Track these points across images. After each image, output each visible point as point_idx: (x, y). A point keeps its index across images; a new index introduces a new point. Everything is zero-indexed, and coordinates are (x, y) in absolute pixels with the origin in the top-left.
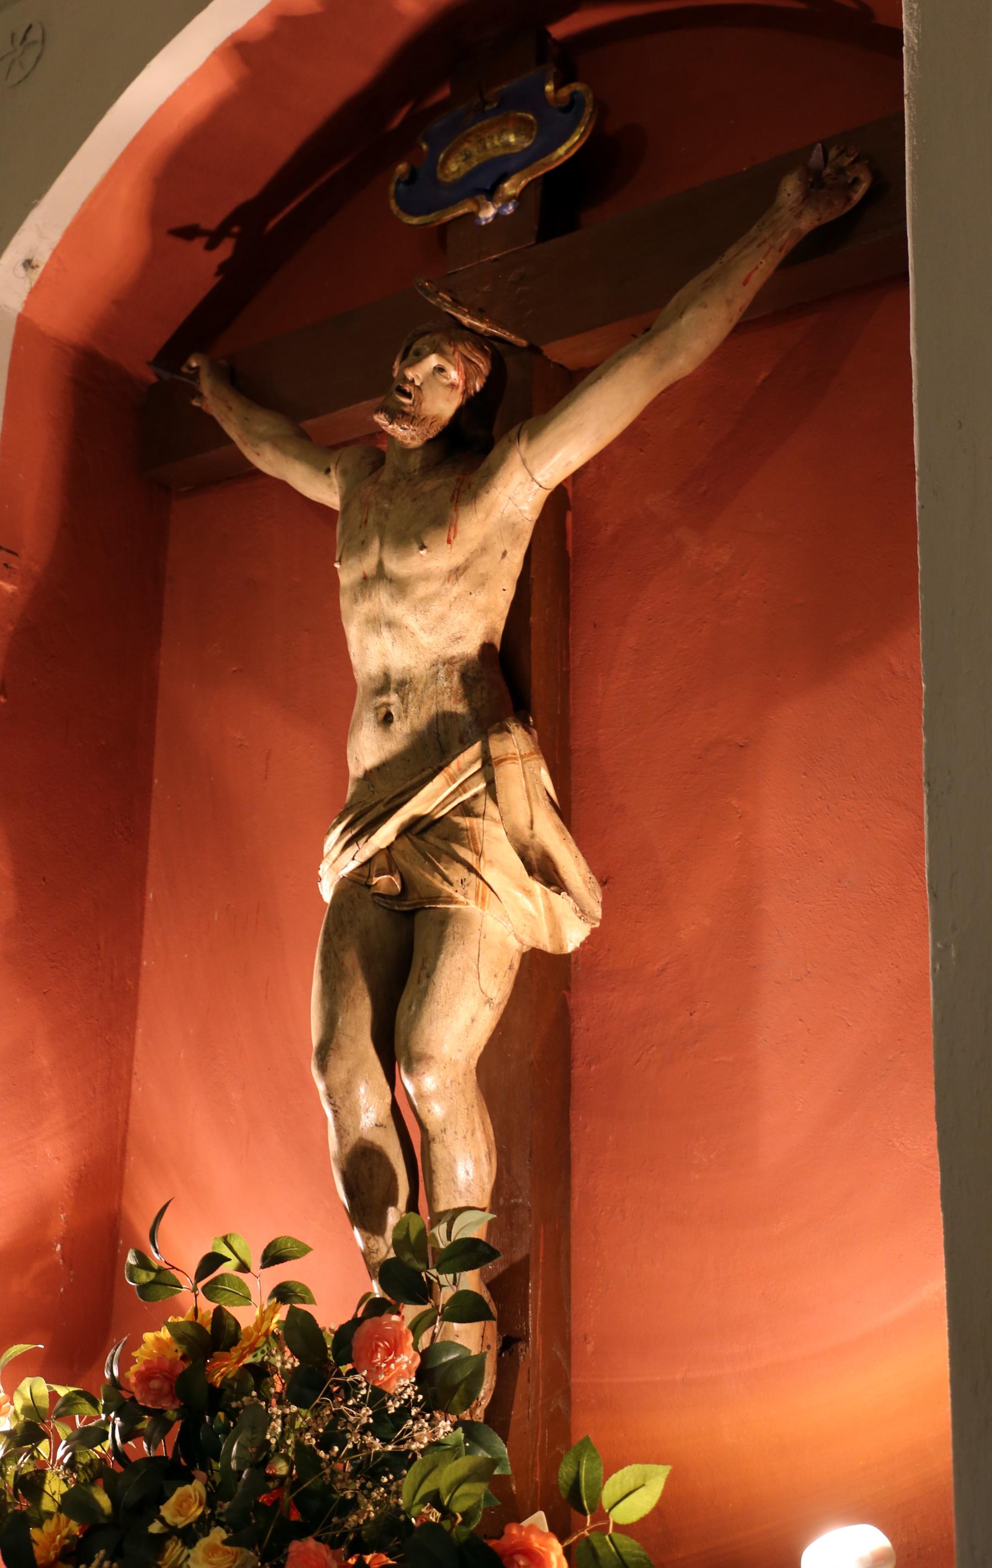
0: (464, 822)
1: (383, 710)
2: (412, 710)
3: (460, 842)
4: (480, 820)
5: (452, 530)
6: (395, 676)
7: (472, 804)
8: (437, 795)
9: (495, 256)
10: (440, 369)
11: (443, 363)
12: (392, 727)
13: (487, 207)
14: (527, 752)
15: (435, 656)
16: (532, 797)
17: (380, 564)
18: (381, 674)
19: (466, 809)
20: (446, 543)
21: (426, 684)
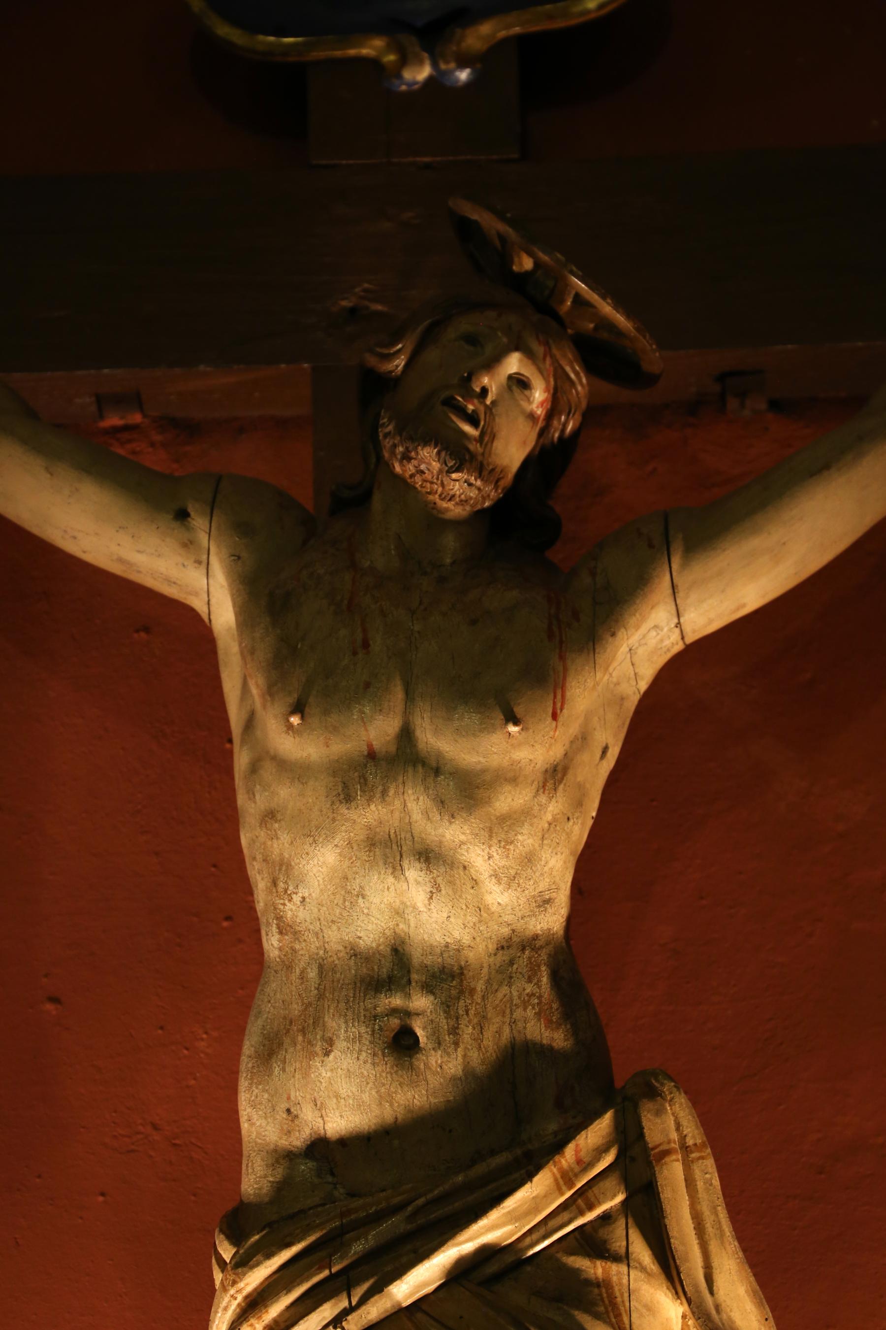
0: (596, 1269)
1: (395, 1022)
2: (467, 1032)
3: (590, 1308)
4: (624, 1268)
5: (559, 697)
6: (417, 957)
7: (603, 1233)
8: (537, 1210)
9: (427, 159)
10: (520, 383)
11: (528, 371)
12: (420, 1061)
13: (421, 63)
14: (699, 1141)
15: (505, 931)
16: (710, 1229)
17: (406, 735)
18: (385, 950)
19: (591, 1242)
20: (550, 719)
21: (489, 982)
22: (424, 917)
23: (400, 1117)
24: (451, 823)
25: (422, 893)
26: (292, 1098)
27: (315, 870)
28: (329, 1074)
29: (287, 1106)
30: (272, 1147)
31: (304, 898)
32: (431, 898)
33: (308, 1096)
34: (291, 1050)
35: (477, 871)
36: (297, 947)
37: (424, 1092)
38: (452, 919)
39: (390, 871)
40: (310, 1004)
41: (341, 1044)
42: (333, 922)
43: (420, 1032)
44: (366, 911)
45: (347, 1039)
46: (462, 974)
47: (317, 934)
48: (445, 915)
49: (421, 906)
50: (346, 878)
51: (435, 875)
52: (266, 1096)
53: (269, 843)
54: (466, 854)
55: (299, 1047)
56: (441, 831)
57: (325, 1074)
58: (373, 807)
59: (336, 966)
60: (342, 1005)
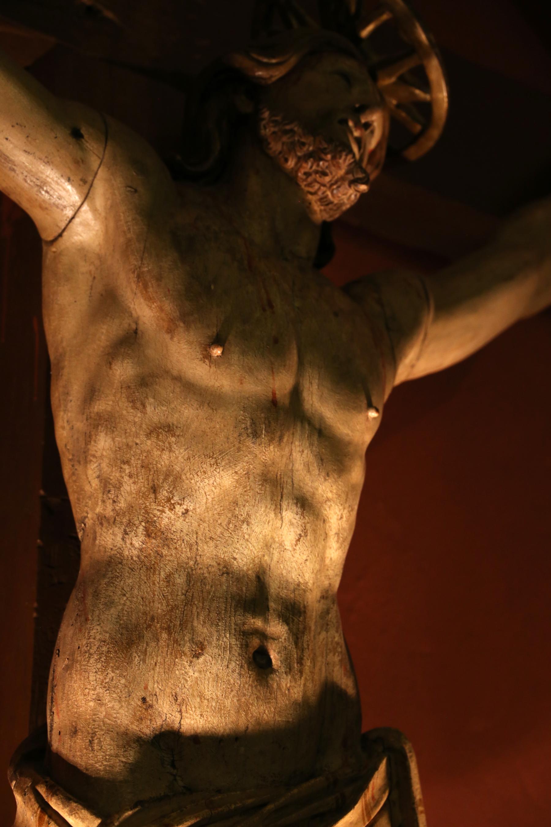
1: (255, 642)
6: (273, 588)
17: (296, 393)
22: (288, 555)
23: (250, 727)
24: (325, 480)
25: (292, 533)
26: (149, 688)
27: (207, 489)
28: (197, 674)
29: (144, 695)
30: (122, 729)
31: (187, 511)
32: (299, 540)
33: (168, 690)
34: (153, 644)
35: (330, 527)
36: (165, 552)
37: (273, 709)
38: (308, 563)
39: (273, 507)
40: (177, 607)
41: (212, 650)
42: (211, 538)
43: (274, 656)
44: (246, 537)
45: (218, 646)
46: (305, 612)
47: (191, 546)
48: (305, 557)
49: (288, 545)
50: (236, 503)
51: (306, 521)
52: (123, 681)
53: (156, 453)
54: (328, 509)
55: (162, 643)
56: (316, 484)
57: (192, 673)
58: (272, 447)
59: (205, 578)
60: (213, 615)
